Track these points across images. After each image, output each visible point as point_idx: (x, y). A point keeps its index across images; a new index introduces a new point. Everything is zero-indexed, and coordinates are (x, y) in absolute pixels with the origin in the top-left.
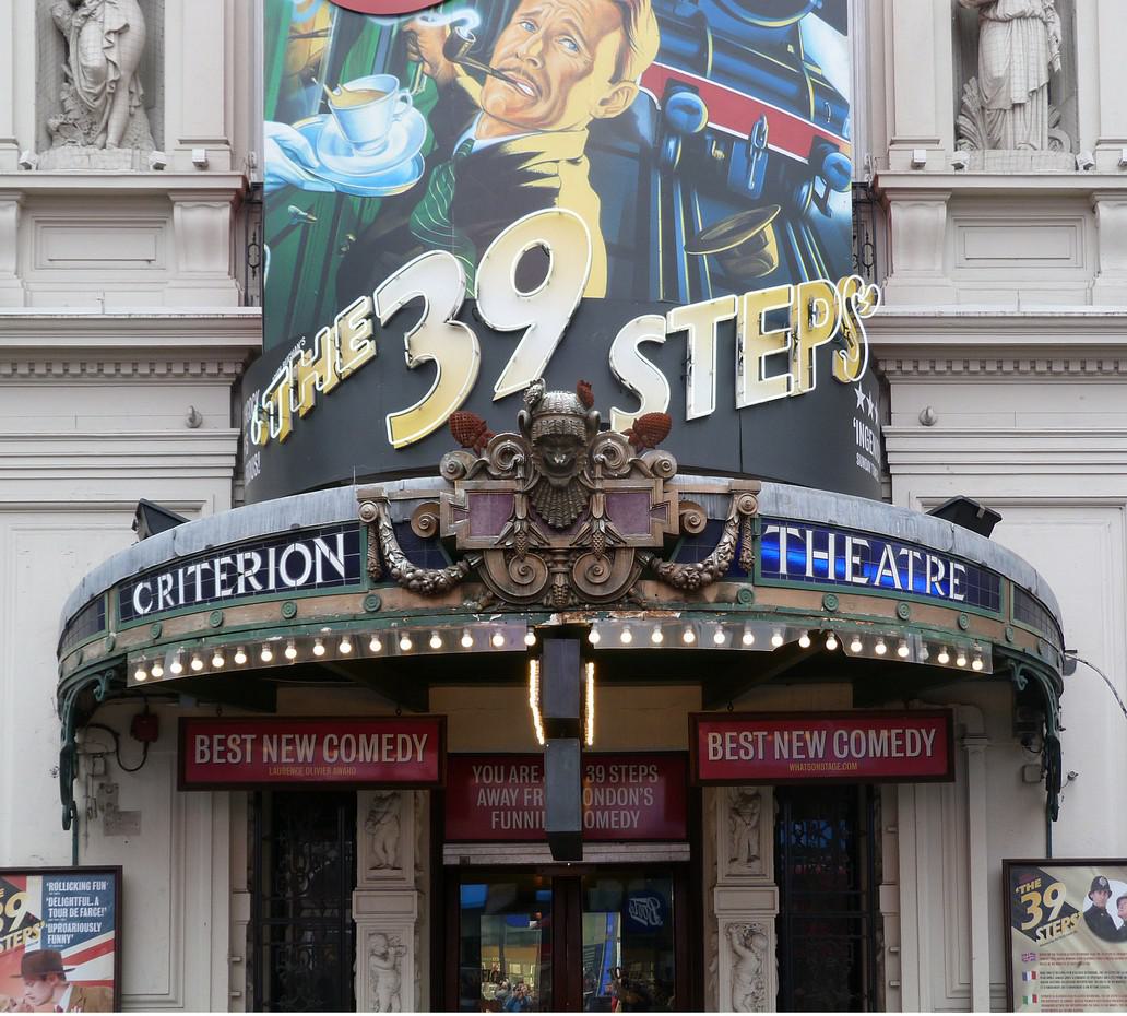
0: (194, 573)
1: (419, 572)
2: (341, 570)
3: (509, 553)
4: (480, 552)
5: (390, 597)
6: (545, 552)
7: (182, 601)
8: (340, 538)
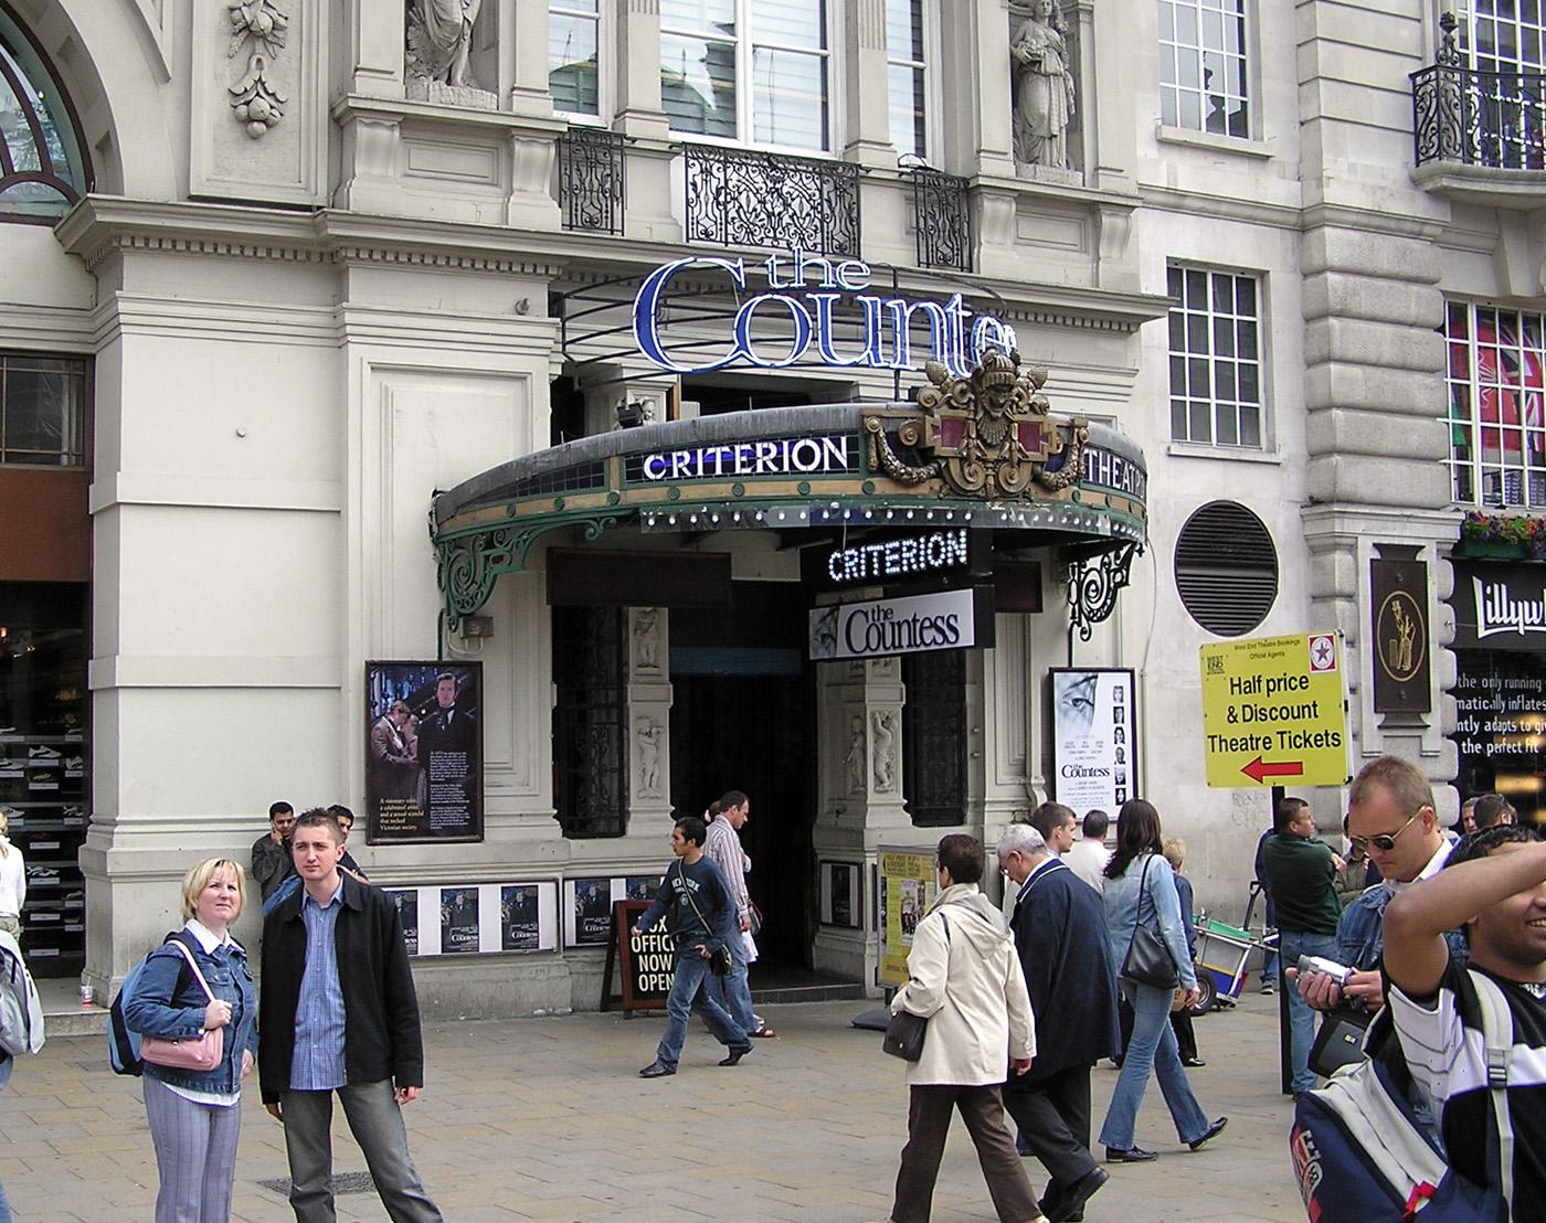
0: (714, 454)
1: (909, 469)
2: (844, 463)
3: (962, 460)
4: (946, 458)
5: (881, 486)
7: (700, 473)
8: (844, 439)
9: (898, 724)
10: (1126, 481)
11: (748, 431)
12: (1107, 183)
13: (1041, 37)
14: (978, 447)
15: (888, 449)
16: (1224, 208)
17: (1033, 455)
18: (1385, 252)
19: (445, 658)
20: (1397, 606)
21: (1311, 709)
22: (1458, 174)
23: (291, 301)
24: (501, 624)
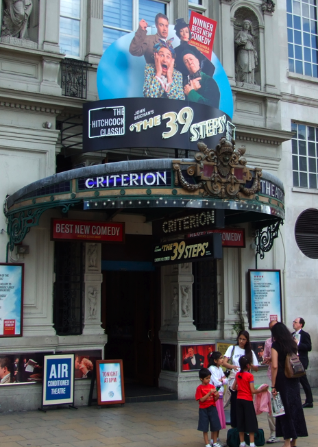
0: (113, 178)
2: (165, 182)
3: (212, 182)
5: (180, 191)
6: (220, 182)
7: (108, 185)
8: (165, 173)
9: (191, 291)
10: (277, 194)
12: (269, 90)
13: (245, 37)
14: (218, 177)
15: (182, 177)
16: (311, 102)
17: (240, 181)
19: (9, 262)
24: (33, 248)
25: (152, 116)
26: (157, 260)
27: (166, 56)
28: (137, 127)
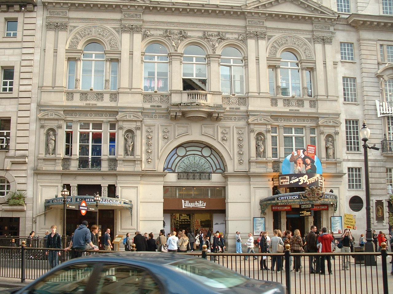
5: (302, 200)
9: (313, 223)
11: (288, 195)
12: (338, 160)
13: (329, 144)
18: (377, 164)
20: (379, 207)
21: (352, 222)
22: (386, 154)
23: (245, 181)
25: (296, 179)
26: (301, 215)
27: (300, 161)
28: (292, 182)
